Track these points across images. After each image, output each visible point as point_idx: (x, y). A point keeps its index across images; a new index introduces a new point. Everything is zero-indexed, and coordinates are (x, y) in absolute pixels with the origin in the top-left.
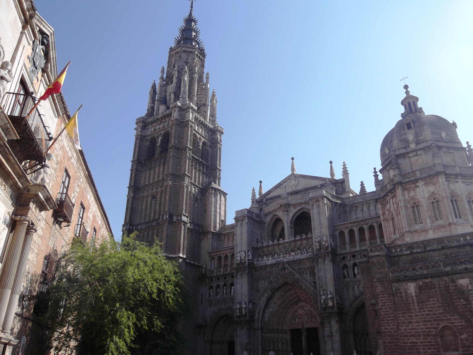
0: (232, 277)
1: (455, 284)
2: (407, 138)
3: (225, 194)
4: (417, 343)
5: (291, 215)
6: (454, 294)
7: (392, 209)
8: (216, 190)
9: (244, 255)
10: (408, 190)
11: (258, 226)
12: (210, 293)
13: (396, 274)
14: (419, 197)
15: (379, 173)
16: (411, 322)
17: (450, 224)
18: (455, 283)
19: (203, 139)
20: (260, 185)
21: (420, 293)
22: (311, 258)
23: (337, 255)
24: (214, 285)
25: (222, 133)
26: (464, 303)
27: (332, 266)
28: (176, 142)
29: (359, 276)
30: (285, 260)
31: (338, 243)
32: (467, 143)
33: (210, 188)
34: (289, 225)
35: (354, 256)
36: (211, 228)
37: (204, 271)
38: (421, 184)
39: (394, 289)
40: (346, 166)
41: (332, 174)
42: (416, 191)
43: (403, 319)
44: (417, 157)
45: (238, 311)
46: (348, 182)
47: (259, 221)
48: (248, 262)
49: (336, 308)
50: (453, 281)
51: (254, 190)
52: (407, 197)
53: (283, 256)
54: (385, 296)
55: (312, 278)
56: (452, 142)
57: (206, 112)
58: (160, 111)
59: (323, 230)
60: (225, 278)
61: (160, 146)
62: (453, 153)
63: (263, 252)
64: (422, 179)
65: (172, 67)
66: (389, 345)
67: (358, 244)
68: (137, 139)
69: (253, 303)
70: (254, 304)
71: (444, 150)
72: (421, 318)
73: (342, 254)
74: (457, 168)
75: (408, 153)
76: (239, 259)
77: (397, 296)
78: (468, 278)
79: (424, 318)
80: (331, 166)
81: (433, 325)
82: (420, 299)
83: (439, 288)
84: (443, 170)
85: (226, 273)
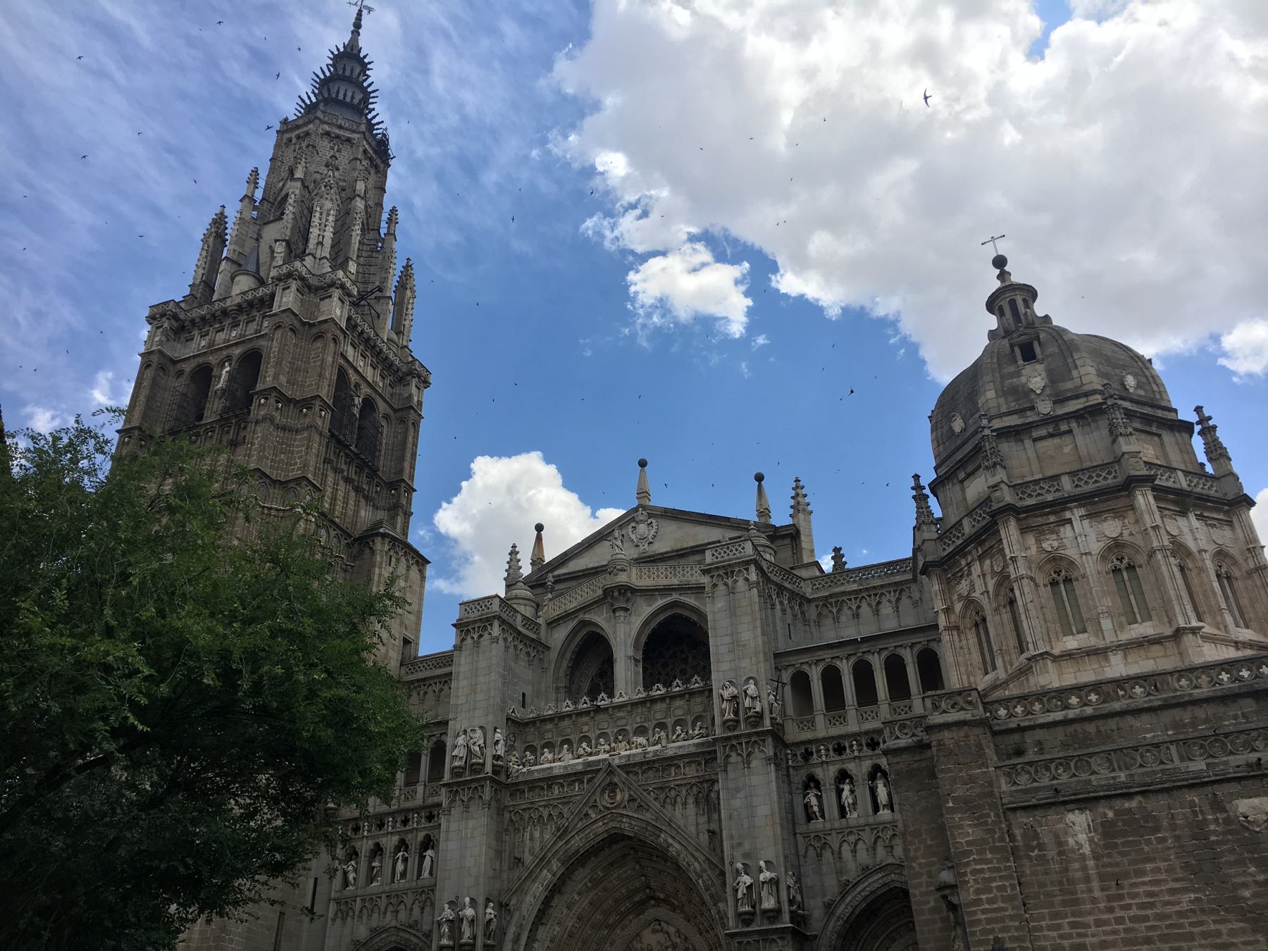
0: (430, 818)
1: (1225, 815)
2: (1024, 385)
3: (422, 562)
5: (637, 622)
7: (976, 595)
10: (1040, 531)
11: (528, 654)
12: (345, 873)
14: (1071, 553)
15: (927, 491)
17: (1178, 633)
18: (1227, 811)
19: (365, 390)
20: (539, 539)
21: (1106, 846)
22: (703, 753)
23: (786, 746)
24: (365, 847)
25: (426, 383)
26: (1261, 877)
27: (773, 774)
28: (283, 379)
29: (855, 815)
31: (790, 711)
32: (1198, 410)
33: (378, 534)
34: (630, 652)
35: (840, 750)
38: (1076, 514)
39: (1018, 832)
40: (804, 492)
41: (764, 513)
42: (1062, 535)
43: (1055, 934)
44: (1056, 441)
45: (445, 929)
46: (810, 535)
48: (493, 766)
49: (786, 917)
50: (1218, 806)
51: (514, 552)
52: (1034, 549)
53: (607, 747)
54: (989, 856)
55: (703, 819)
56: (1153, 406)
58: (236, 290)
59: (745, 663)
60: (405, 822)
61: (223, 391)
62: (1159, 436)
64: (1080, 499)
65: (284, 174)
67: (851, 713)
68: (146, 365)
69: (501, 905)
70: (503, 907)
72: (1114, 932)
73: (802, 743)
74: (1180, 473)
76: (461, 752)
77: (1029, 857)
79: (1126, 930)
80: (760, 487)
82: (1110, 865)
83: (1173, 827)
84: (1145, 472)
85: (409, 804)
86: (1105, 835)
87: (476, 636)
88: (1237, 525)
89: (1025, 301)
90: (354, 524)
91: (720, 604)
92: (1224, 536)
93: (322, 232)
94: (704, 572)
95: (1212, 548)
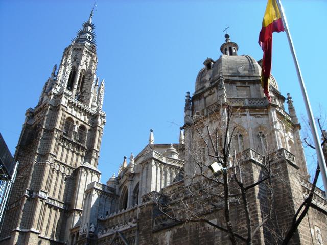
6: (202, 239)
8: (86, 169)
9: (86, 227)
13: (159, 223)
19: (80, 123)
25: (104, 117)
30: (120, 230)
34: (132, 194)
36: (76, 206)
39: (153, 240)
47: (111, 194)
57: (89, 99)
62: (249, 87)
63: (109, 225)
68: (24, 128)
71: (239, 84)
75: (203, 93)
78: (216, 217)
83: (190, 233)
87: (89, 195)
88: (269, 115)
90: (76, 165)
91: (144, 174)
92: (263, 121)
95: (256, 126)
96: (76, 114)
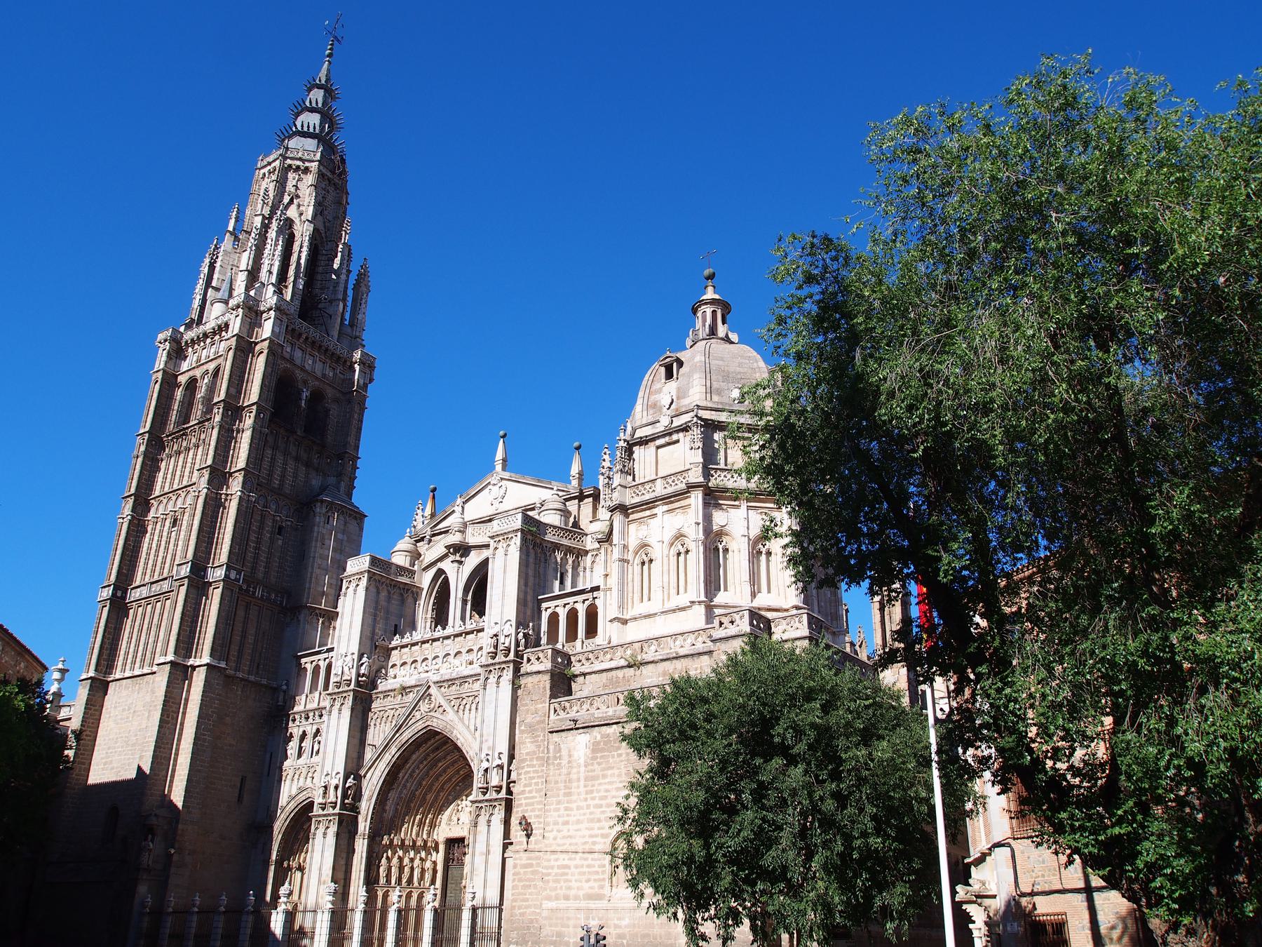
4: (568, 867)
14: (652, 541)
16: (567, 823)
19: (313, 383)
21: (594, 758)
30: (436, 678)
37: (281, 698)
39: (551, 747)
66: (522, 871)
81: (602, 828)
86: (594, 751)
89: (714, 312)
93: (270, 261)
94: (492, 537)
96: (304, 360)
